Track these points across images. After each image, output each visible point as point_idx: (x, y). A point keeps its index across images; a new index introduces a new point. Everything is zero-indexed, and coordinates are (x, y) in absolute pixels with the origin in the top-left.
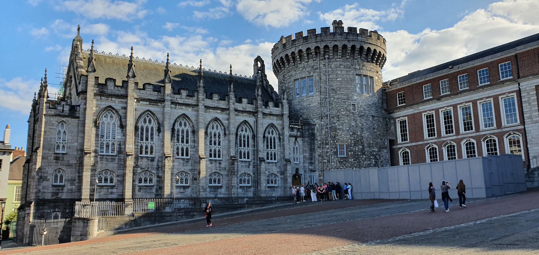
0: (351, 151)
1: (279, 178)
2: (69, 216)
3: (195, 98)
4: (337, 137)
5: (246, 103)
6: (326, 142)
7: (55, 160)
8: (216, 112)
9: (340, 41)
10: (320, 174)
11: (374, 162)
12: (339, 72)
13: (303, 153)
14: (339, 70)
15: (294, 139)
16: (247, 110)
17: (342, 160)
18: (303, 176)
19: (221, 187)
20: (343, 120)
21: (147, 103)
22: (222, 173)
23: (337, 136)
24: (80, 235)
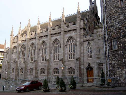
5: (57, 28)
15: (87, 43)
16: (58, 32)
17: (114, 53)
20: (114, 17)
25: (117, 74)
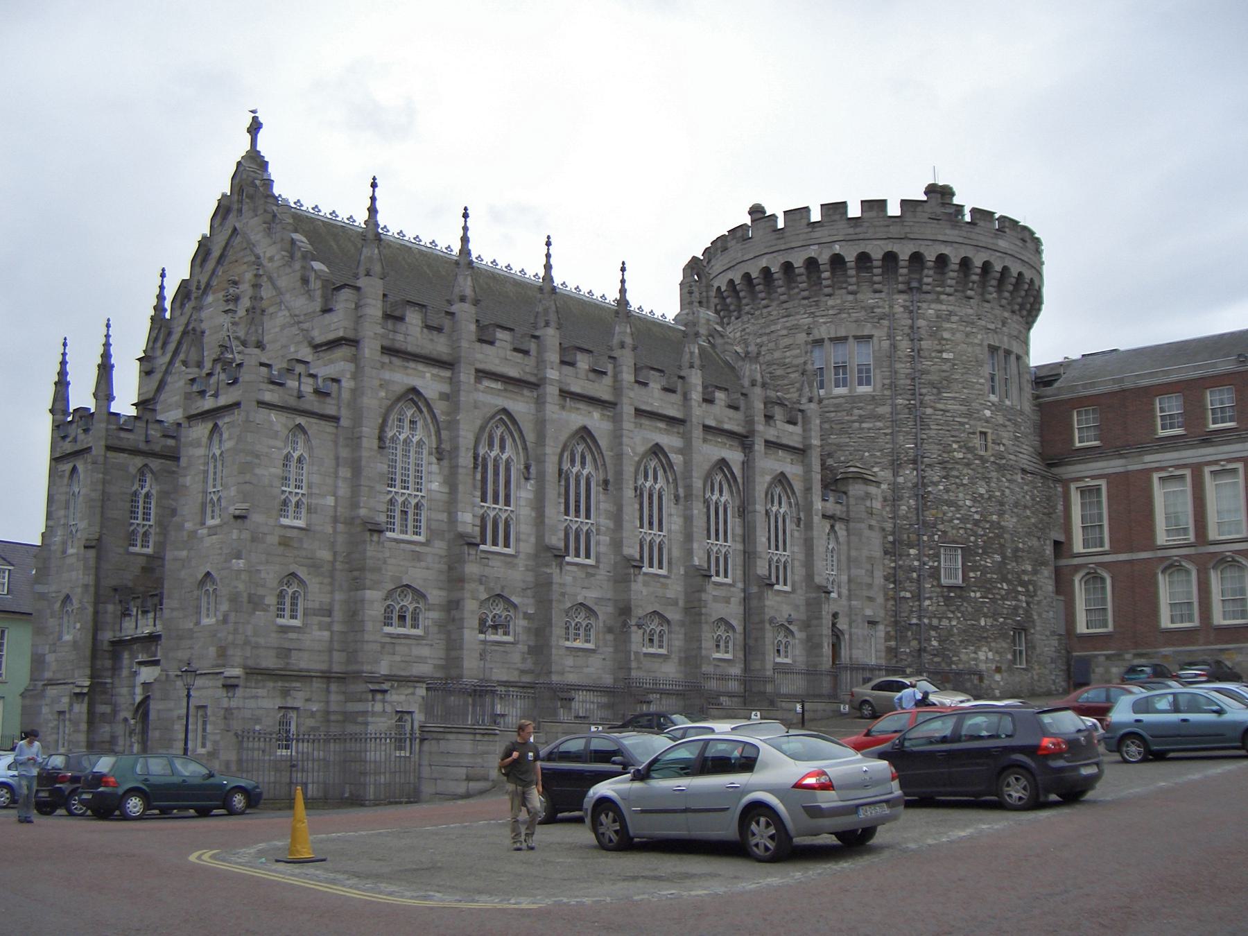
0: (973, 569)
1: (797, 641)
2: (318, 725)
3: (607, 380)
4: (941, 527)
6: (909, 537)
7: (282, 548)
8: (656, 427)
9: (955, 245)
10: (887, 633)
11: (1024, 605)
12: (946, 335)
13: (849, 568)
14: (945, 330)
16: (726, 426)
17: (952, 594)
18: (847, 636)
19: (665, 658)
20: (957, 477)
21: (499, 386)
22: (669, 616)
23: (943, 523)
24: (464, 777)
25: (960, 660)
